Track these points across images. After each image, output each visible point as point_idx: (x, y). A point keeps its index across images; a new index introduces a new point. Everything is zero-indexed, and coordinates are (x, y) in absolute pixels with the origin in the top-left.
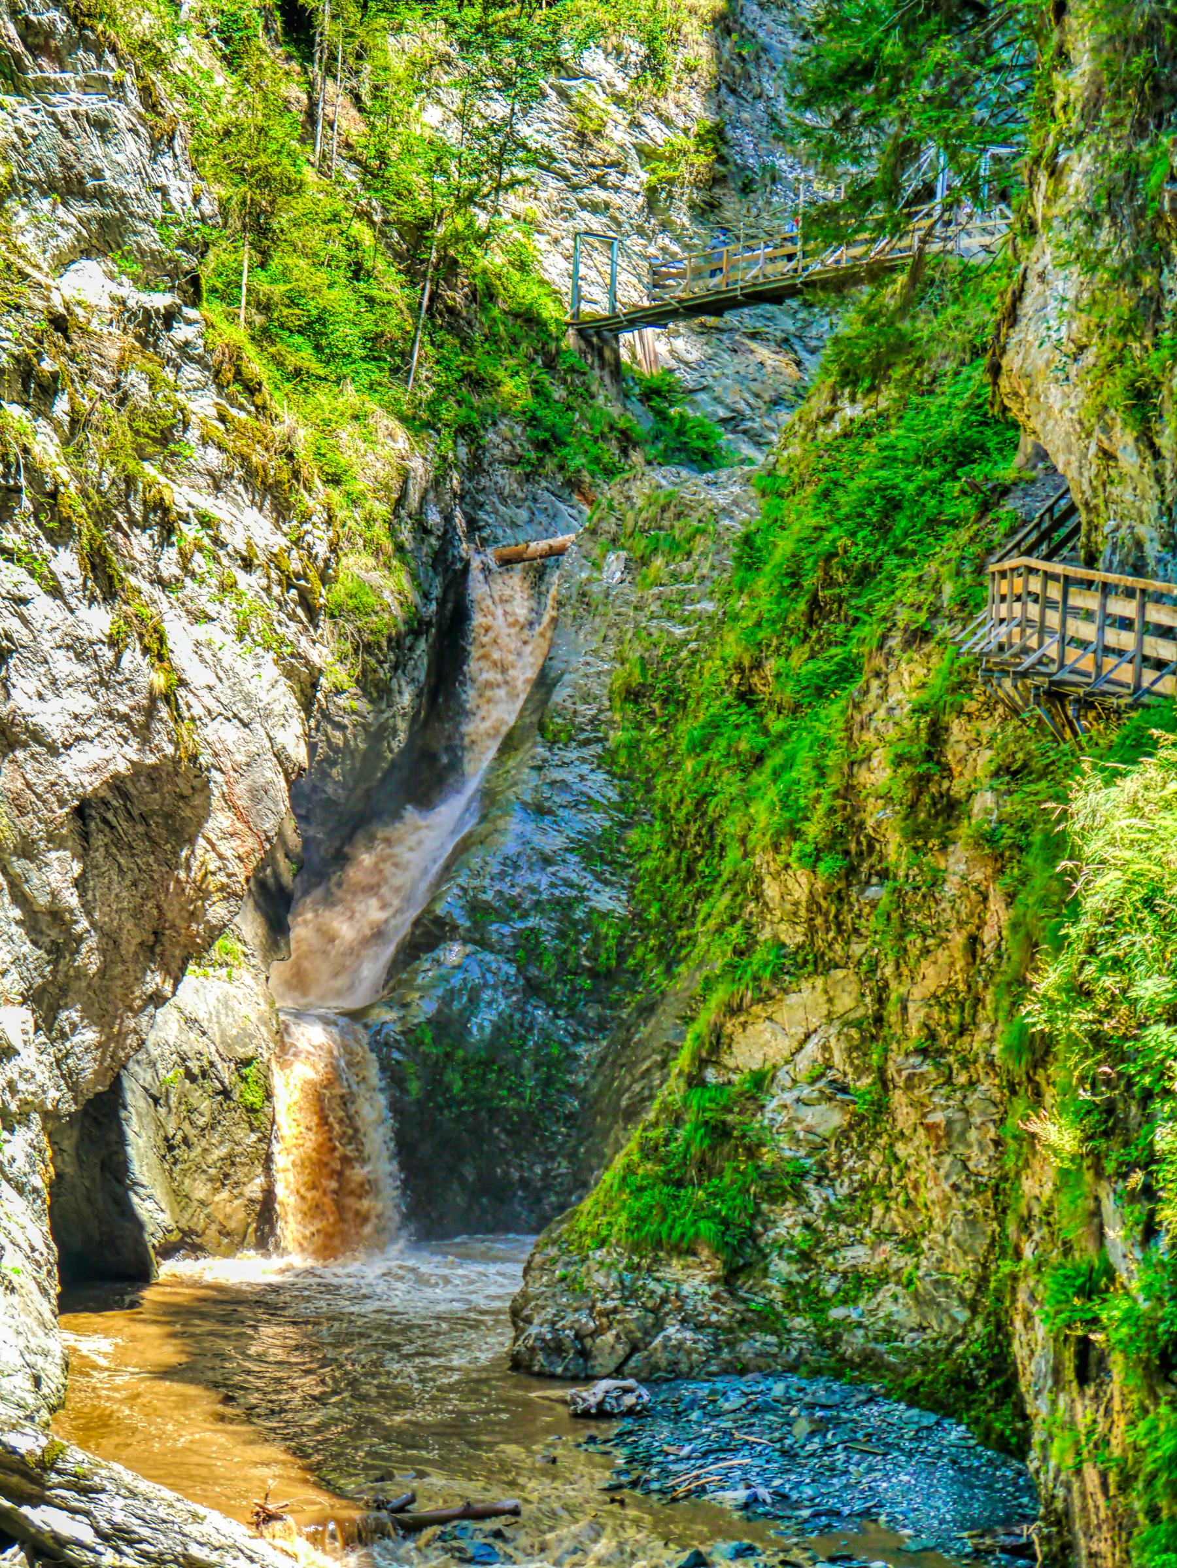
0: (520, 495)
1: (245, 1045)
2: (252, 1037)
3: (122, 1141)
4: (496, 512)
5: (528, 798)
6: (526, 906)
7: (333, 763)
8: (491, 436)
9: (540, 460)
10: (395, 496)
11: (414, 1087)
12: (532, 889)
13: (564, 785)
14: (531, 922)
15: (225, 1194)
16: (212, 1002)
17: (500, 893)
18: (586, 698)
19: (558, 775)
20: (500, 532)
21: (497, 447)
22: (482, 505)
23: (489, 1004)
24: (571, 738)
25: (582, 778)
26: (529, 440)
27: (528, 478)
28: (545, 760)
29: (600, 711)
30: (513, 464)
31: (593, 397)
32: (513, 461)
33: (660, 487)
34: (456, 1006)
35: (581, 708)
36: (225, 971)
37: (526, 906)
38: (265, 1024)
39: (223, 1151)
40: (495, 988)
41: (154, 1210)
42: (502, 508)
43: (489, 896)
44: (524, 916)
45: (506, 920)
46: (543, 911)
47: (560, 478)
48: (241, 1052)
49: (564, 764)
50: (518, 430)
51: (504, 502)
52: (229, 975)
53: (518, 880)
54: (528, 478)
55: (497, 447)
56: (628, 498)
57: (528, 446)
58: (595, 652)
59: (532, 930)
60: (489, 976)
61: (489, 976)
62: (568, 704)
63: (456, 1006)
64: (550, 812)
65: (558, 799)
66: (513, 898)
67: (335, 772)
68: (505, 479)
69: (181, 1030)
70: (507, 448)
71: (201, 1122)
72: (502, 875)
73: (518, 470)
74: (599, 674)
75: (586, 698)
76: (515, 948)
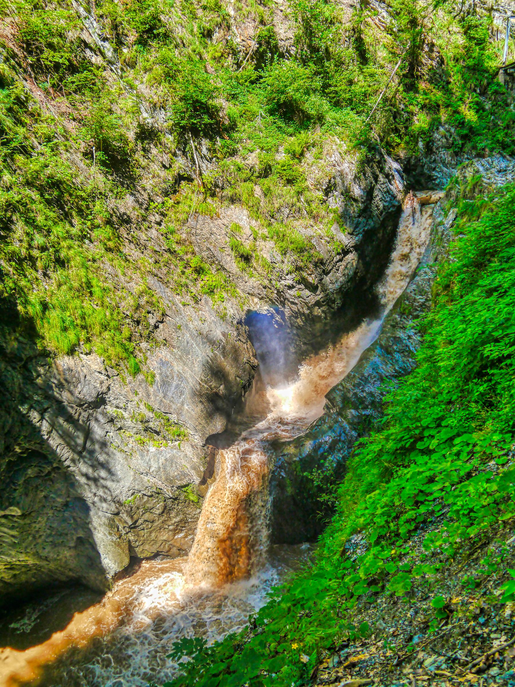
0: (453, 162)
1: (181, 480)
2: (185, 475)
3: (90, 534)
4: (442, 171)
5: (383, 343)
6: (367, 403)
7: (297, 318)
8: (436, 135)
9: (463, 145)
10: (324, 188)
11: (290, 490)
12: (371, 394)
13: (398, 340)
14: (368, 412)
15: (181, 535)
16: (162, 460)
17: (355, 394)
18: (421, 292)
19: (400, 334)
20: (444, 180)
21: (439, 140)
22: (434, 169)
23: (339, 451)
24: (410, 313)
25: (409, 337)
26: (458, 135)
27: (456, 154)
28: (397, 323)
29: (426, 300)
30: (449, 148)
31: (507, 105)
32: (448, 147)
33: (478, 172)
34: (321, 451)
35: (417, 297)
36: (177, 443)
37: (367, 403)
38: (194, 469)
39: (178, 519)
40: (344, 442)
41: (111, 562)
42: (445, 169)
43: (350, 395)
44: (365, 408)
45: (356, 409)
46: (375, 407)
47: (474, 153)
48: (178, 483)
49: (404, 328)
50: (453, 130)
51: (445, 165)
52: (179, 445)
53: (366, 389)
54: (456, 154)
55: (439, 140)
56: (465, 177)
57: (457, 138)
58: (430, 267)
59: (368, 416)
60: (343, 435)
61: (343, 435)
62: (412, 295)
63: (321, 451)
64: (389, 353)
65: (395, 347)
66: (361, 398)
67: (299, 320)
68: (446, 155)
69: (135, 480)
70: (444, 140)
71: (158, 512)
72: (359, 385)
73: (451, 151)
74: (429, 279)
75: (421, 292)
76: (359, 423)
